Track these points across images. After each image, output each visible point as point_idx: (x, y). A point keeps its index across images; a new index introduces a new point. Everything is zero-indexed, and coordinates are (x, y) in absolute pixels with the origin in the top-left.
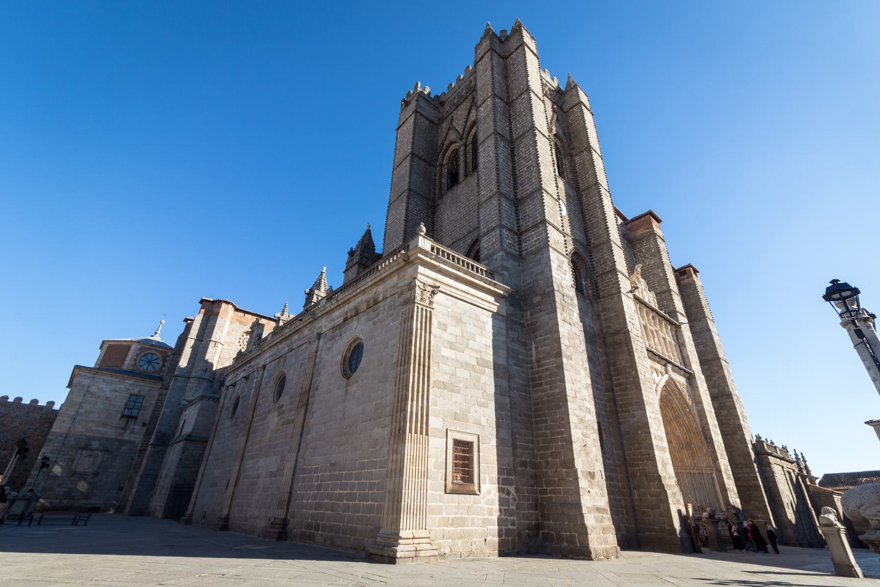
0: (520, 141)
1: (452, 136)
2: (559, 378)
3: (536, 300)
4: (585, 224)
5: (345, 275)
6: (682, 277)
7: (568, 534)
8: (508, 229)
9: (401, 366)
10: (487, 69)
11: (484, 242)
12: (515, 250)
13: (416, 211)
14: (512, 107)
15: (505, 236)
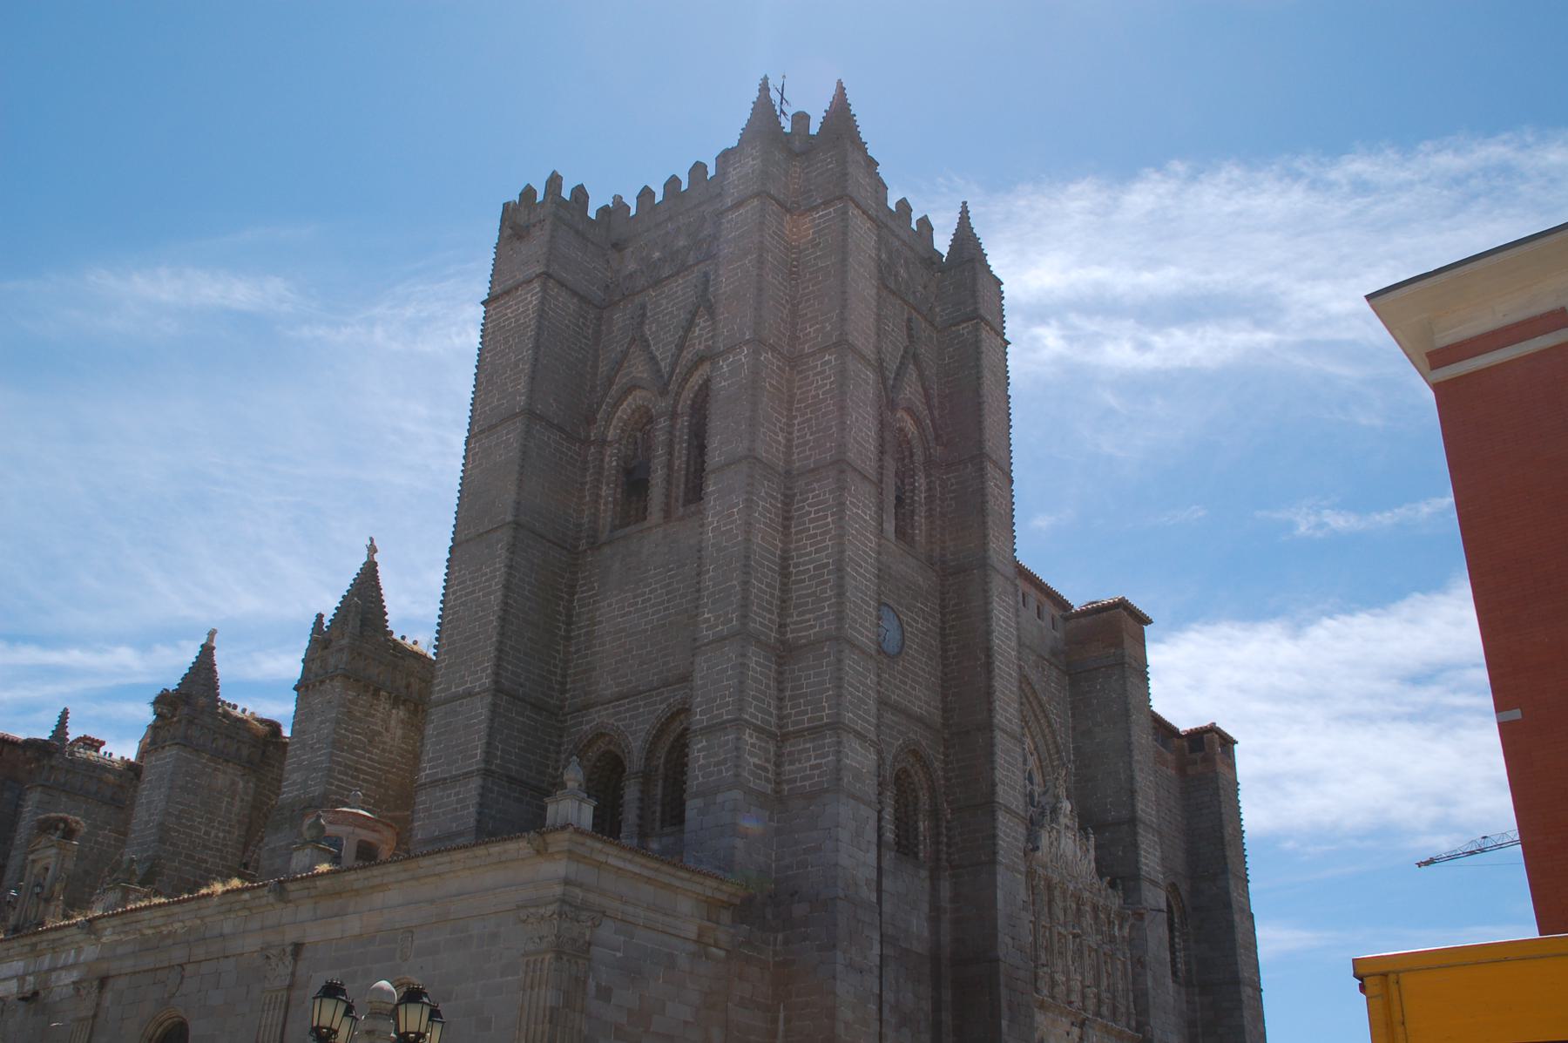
0: (807, 484)
1: (638, 369)
8: (757, 729)
11: (699, 751)
12: (768, 780)
13: (528, 588)
14: (799, 372)
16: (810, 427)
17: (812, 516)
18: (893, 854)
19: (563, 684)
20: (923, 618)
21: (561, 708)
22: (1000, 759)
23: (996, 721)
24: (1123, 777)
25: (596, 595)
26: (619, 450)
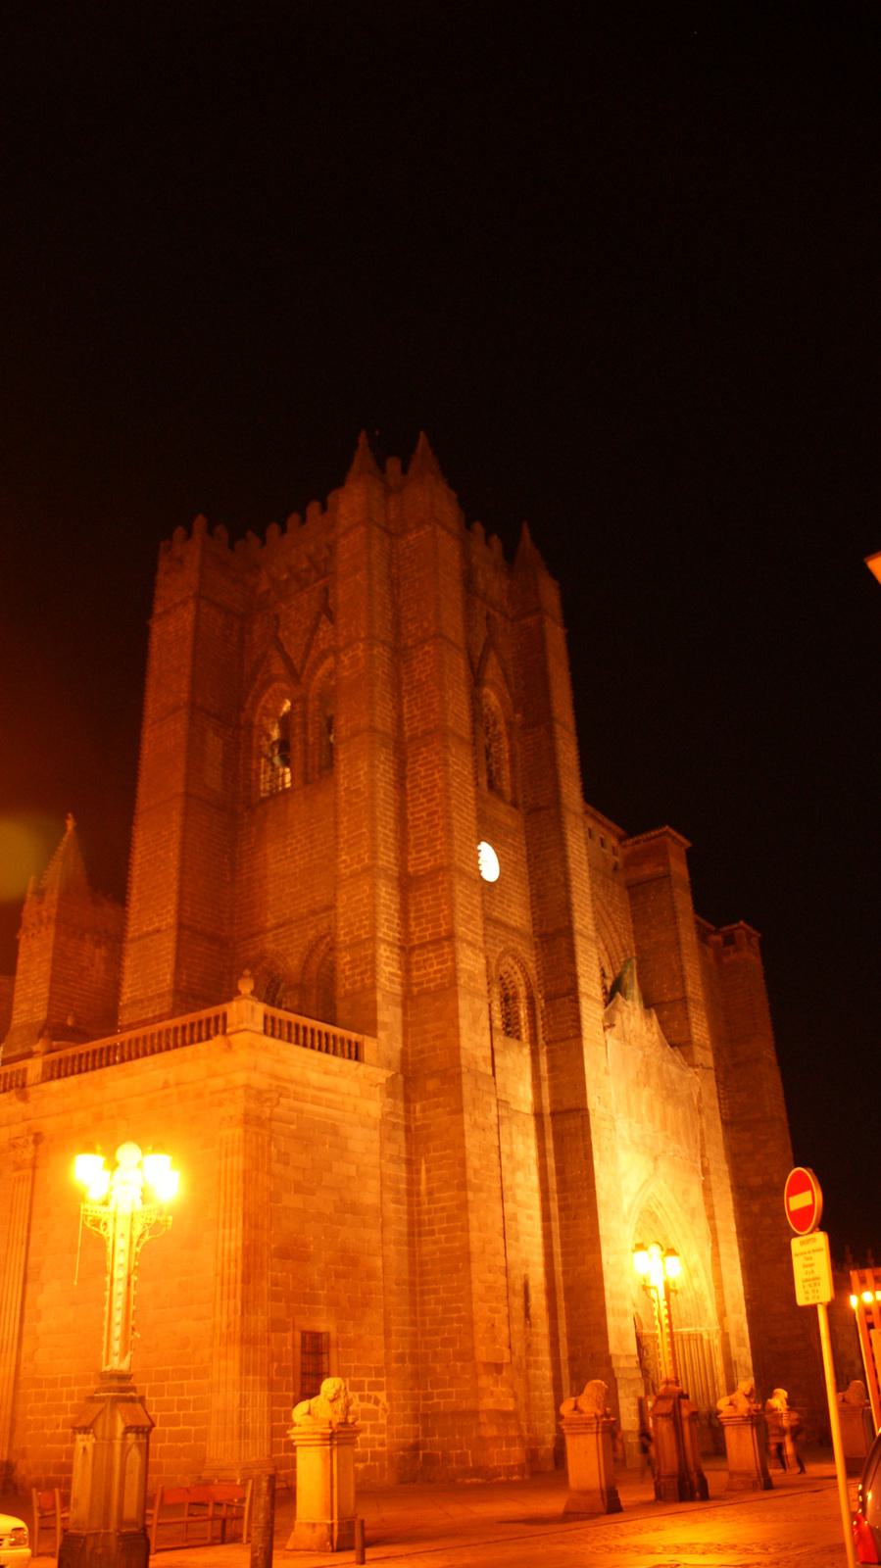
2: (459, 1224)
7: (459, 1451)
9: (224, 1227)
14: (405, 662)
16: (416, 704)
18: (502, 1037)
22: (581, 958)
23: (575, 928)
24: (675, 967)
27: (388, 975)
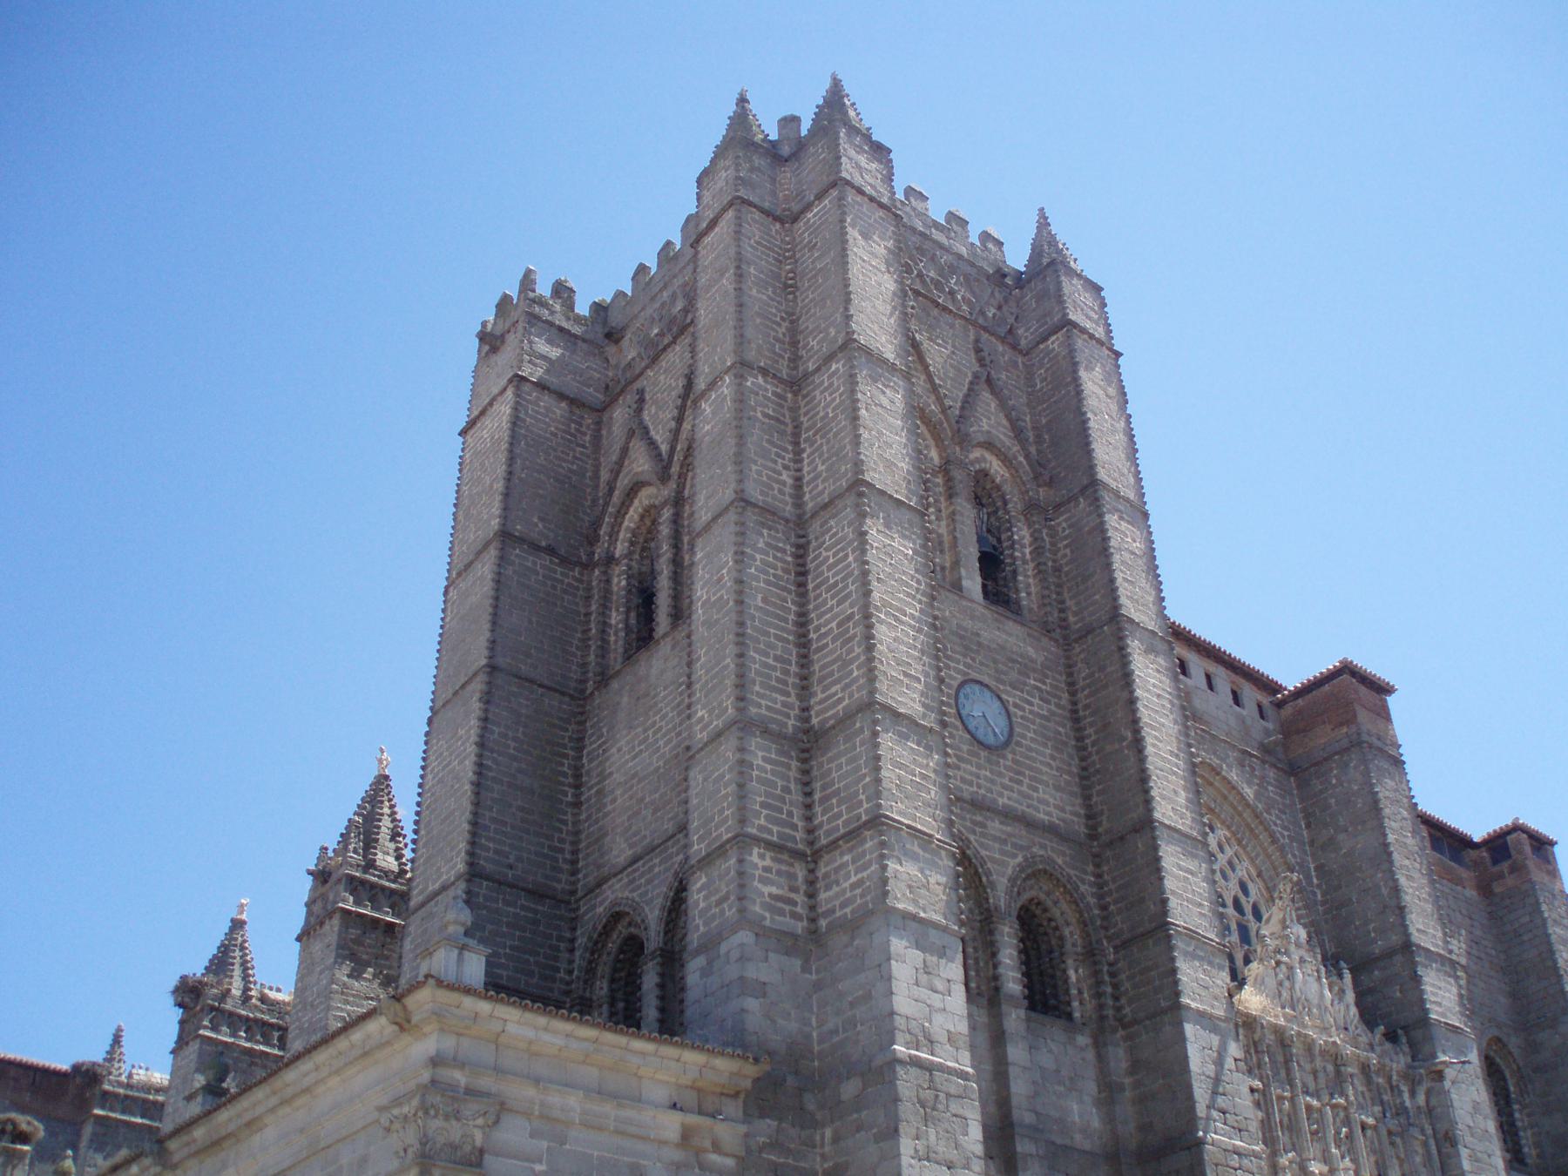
1: (640, 463)
3: (850, 1089)
4: (1082, 759)
5: (303, 950)
6: (1497, 869)
10: (727, 270)
11: (699, 891)
12: (794, 916)
13: (513, 744)
14: (804, 397)
15: (757, 873)
17: (831, 561)
18: (1022, 1013)
19: (574, 862)
20: (1041, 699)
21: (573, 893)
23: (1157, 815)
25: (604, 743)
26: (630, 568)
27: (768, 899)
